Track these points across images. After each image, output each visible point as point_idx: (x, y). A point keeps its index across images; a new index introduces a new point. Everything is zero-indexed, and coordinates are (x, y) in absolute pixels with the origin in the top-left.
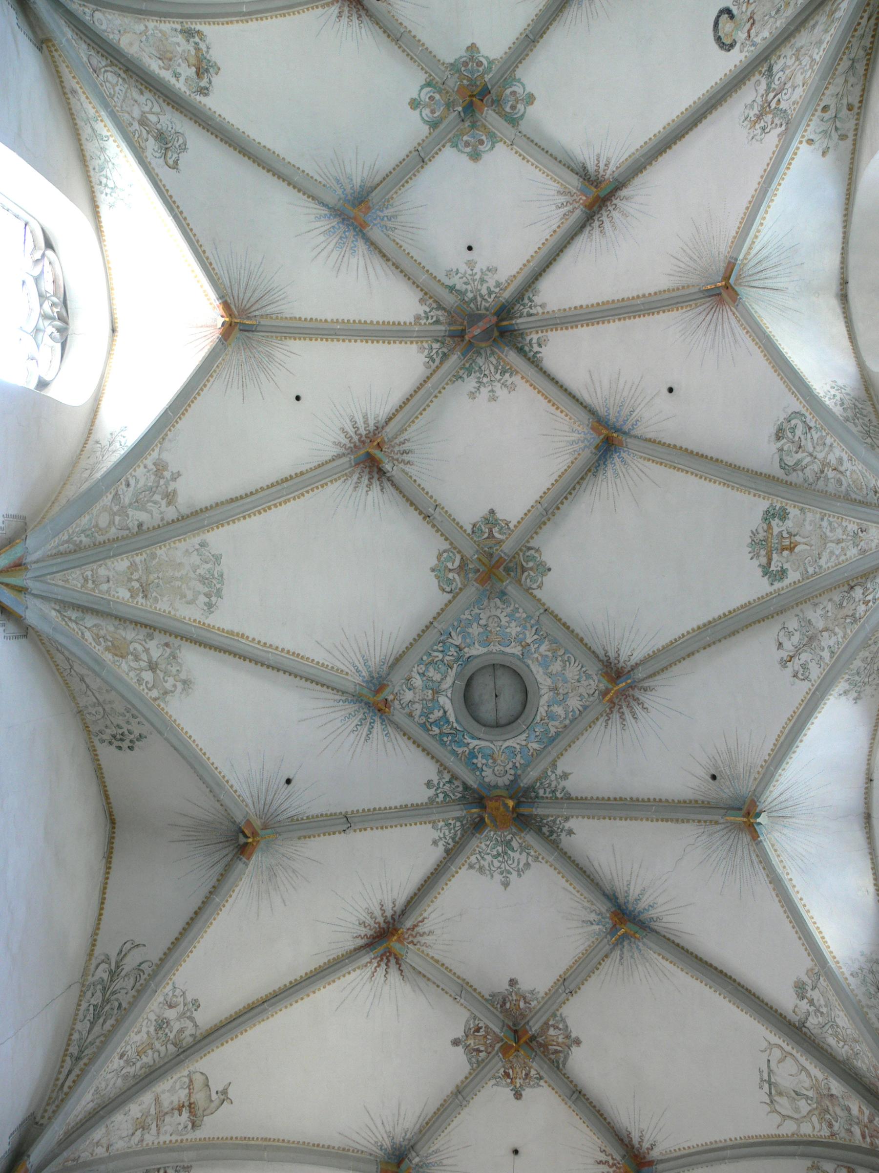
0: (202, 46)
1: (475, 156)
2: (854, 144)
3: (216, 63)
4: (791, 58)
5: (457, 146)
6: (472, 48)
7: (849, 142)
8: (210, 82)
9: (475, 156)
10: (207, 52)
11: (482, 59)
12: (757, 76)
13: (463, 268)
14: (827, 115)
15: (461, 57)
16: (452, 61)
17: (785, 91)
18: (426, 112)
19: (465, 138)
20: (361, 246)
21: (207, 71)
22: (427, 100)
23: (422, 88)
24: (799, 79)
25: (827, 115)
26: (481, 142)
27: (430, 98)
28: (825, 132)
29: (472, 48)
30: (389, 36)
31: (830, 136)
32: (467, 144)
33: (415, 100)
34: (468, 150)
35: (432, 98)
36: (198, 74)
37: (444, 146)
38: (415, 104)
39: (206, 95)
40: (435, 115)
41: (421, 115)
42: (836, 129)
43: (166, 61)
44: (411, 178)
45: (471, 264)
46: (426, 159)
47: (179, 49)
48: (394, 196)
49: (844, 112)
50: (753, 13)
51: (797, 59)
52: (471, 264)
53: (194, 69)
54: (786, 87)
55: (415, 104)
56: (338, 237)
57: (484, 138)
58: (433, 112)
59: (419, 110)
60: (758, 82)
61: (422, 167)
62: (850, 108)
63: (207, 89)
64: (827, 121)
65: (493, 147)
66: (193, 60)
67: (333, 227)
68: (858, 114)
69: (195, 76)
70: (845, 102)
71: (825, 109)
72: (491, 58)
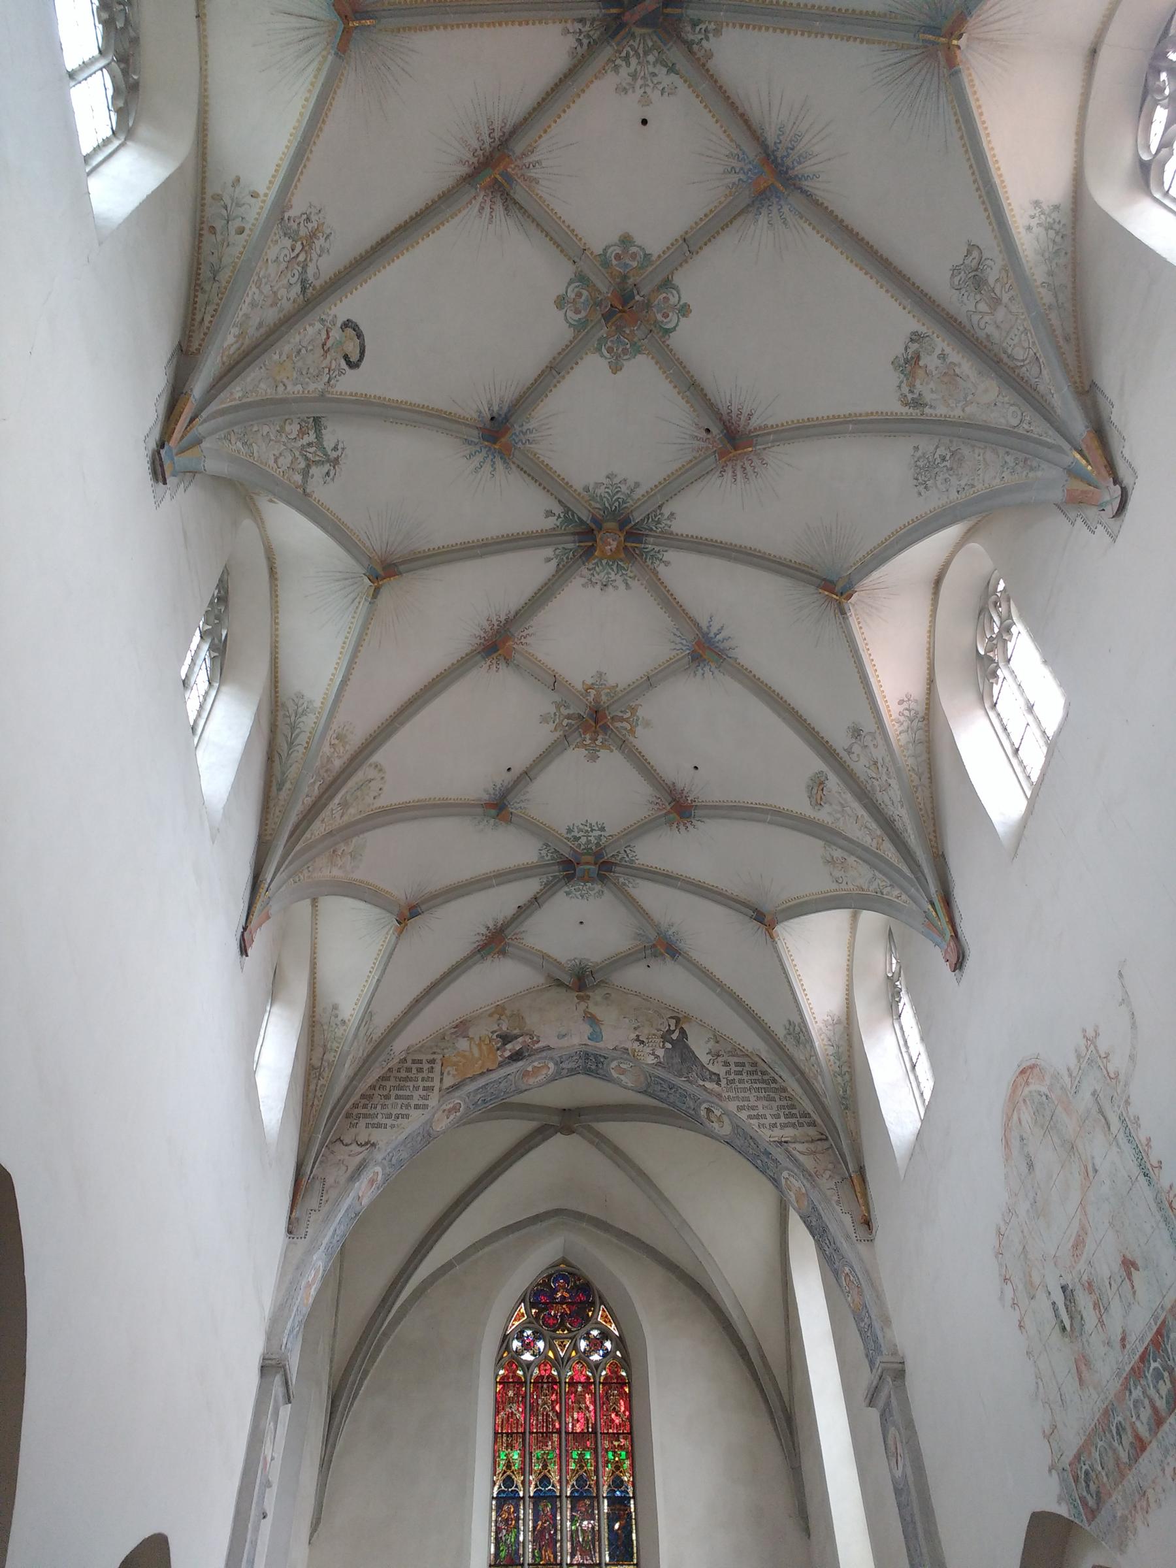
0: (905, 389)
1: (626, 241)
2: (203, 188)
3: (895, 369)
4: (282, 297)
5: (646, 255)
6: (616, 368)
7: (210, 192)
8: (906, 349)
9: (626, 241)
10: (902, 382)
11: (608, 355)
12: (317, 283)
13: (655, 95)
14: (237, 223)
15: (629, 359)
16: (639, 357)
17: (287, 259)
18: (673, 300)
19: (635, 264)
20: (771, 137)
21: (907, 361)
22: (671, 314)
23: (674, 329)
24: (272, 269)
25: (237, 223)
26: (618, 257)
27: (668, 316)
28: (239, 205)
29: (616, 368)
30: (702, 390)
31: (233, 200)
32: (634, 256)
33: (684, 316)
34: (633, 249)
35: (666, 316)
36: (918, 358)
37: (659, 256)
38: (685, 310)
39: (915, 333)
40: (664, 295)
41: (680, 297)
42: (226, 207)
43: (951, 372)
44: (701, 220)
45: (645, 101)
46: (681, 242)
47: (932, 385)
48: (723, 199)
49: (219, 225)
50: (325, 356)
51: (275, 293)
52: (645, 101)
53: (921, 363)
54: (285, 264)
55: (685, 310)
56: (796, 151)
57: (614, 262)
58: (666, 299)
59: (681, 303)
60: (317, 276)
61: (686, 233)
62: (212, 229)
63: (912, 340)
64: (237, 217)
65: (605, 250)
66: (920, 372)
67: (800, 163)
68: (202, 223)
69: (922, 355)
70: (219, 238)
71: (241, 231)
72: (597, 355)
